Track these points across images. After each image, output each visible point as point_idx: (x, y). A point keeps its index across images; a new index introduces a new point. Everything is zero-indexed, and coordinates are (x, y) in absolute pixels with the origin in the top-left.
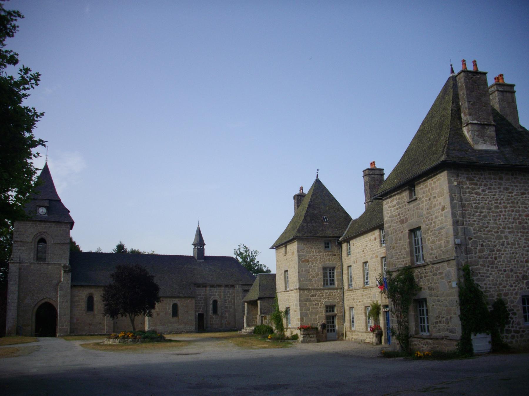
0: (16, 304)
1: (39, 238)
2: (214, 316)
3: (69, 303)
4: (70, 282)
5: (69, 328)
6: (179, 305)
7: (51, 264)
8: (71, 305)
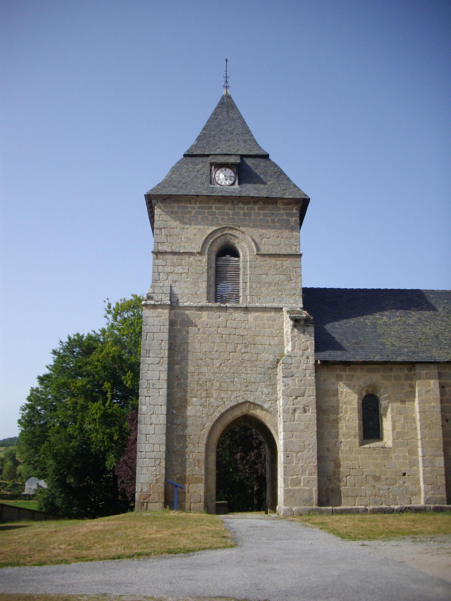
0: (163, 419)
1: (220, 243)
3: (312, 414)
4: (311, 350)
5: (315, 489)
7: (256, 309)
8: (318, 419)
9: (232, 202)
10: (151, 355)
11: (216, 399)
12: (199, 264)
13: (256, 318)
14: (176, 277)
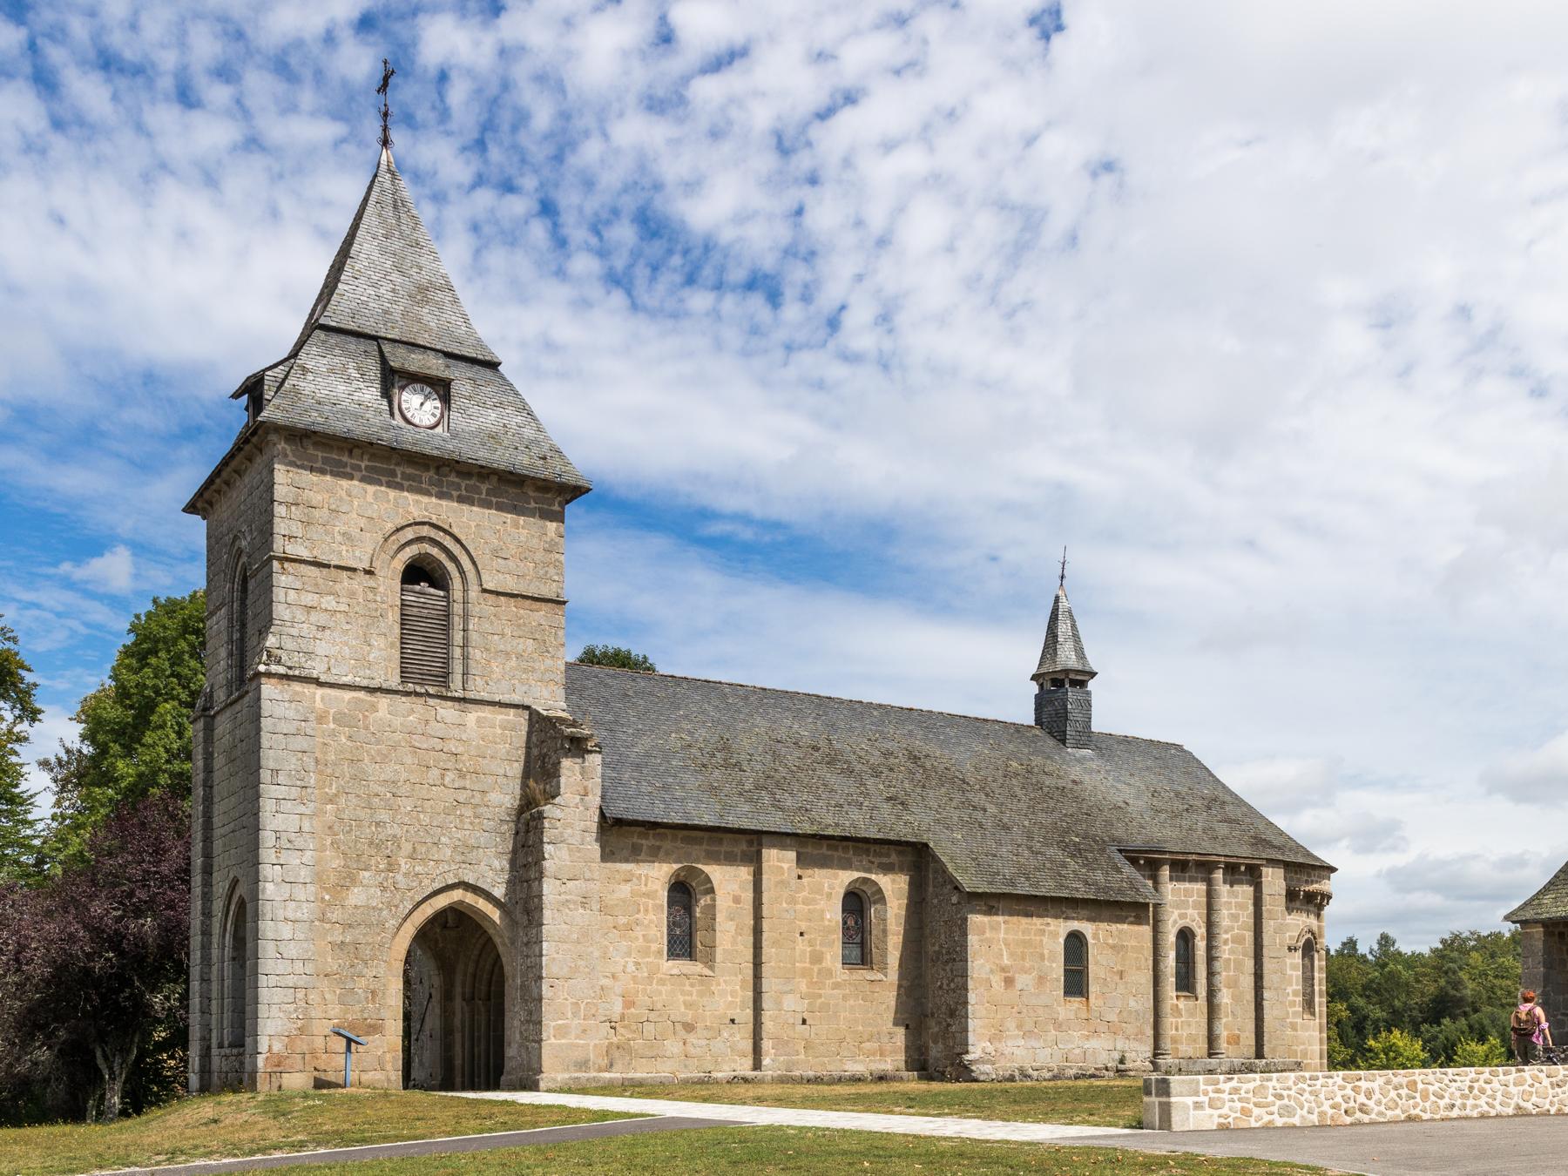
2: (1182, 1004)
6: (1090, 941)
9: (438, 468)
10: (281, 779)
11: (406, 875)
12: (371, 596)
13: (479, 720)
14: (322, 619)
